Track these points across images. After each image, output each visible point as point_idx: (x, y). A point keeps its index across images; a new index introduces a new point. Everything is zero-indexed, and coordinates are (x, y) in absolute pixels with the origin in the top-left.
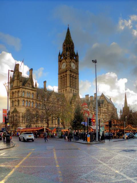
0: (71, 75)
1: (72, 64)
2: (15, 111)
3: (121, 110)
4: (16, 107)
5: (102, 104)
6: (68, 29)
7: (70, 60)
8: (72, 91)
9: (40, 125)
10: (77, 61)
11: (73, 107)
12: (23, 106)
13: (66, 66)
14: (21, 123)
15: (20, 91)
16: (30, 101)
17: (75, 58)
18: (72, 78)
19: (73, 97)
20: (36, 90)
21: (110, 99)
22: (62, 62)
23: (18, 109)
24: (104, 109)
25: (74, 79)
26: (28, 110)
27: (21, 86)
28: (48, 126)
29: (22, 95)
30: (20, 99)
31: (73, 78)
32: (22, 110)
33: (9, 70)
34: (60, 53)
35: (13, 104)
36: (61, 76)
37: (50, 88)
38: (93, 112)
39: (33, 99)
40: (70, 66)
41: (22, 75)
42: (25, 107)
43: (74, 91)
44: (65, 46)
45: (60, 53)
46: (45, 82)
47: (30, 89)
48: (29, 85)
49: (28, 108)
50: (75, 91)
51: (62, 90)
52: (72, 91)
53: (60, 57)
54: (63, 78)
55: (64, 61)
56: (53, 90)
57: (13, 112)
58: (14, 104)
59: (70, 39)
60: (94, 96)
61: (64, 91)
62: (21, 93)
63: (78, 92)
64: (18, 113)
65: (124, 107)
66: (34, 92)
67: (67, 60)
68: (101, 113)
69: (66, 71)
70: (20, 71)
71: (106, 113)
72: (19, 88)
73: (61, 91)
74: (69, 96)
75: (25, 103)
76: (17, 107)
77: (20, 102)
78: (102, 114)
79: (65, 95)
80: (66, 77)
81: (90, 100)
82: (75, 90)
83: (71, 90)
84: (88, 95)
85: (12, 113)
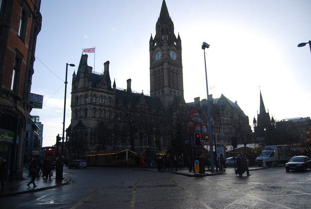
0: (170, 68)
1: (171, 54)
3: (254, 119)
5: (223, 110)
7: (169, 47)
8: (173, 92)
9: (120, 146)
10: (179, 48)
13: (163, 56)
15: (89, 94)
16: (104, 110)
17: (175, 44)
18: (171, 74)
20: (114, 92)
21: (236, 102)
23: (85, 122)
24: (226, 118)
27: (90, 88)
28: (132, 149)
29: (92, 100)
30: (88, 107)
32: (91, 123)
33: (67, 64)
34: (151, 37)
35: (77, 114)
36: (155, 71)
37: (136, 89)
39: (109, 106)
40: (169, 56)
41: (93, 70)
43: (175, 92)
45: (151, 37)
46: (129, 81)
48: (103, 85)
51: (157, 92)
52: (173, 92)
53: (152, 43)
54: (157, 73)
55: (158, 48)
57: (75, 127)
58: (78, 114)
61: (159, 92)
62: (90, 97)
65: (259, 113)
67: (164, 48)
68: (221, 125)
69: (162, 64)
70: (89, 64)
72: (88, 90)
73: (155, 94)
74: (168, 100)
75: (97, 113)
76: (83, 119)
78: (223, 126)
79: (162, 99)
80: (163, 72)
83: (171, 91)
84: (199, 98)
85: (74, 129)
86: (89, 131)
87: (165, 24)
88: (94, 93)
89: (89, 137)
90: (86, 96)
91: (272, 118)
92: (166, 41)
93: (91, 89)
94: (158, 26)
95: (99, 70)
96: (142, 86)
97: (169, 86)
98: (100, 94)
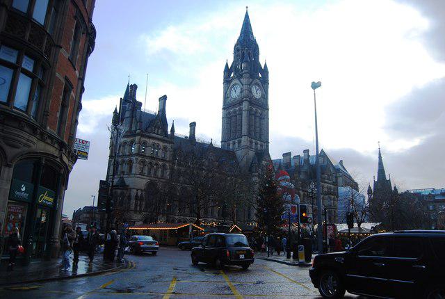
1: (254, 90)
2: (123, 185)
3: (370, 187)
4: (125, 176)
6: (247, 16)
7: (251, 80)
9: (177, 217)
10: (264, 82)
11: (256, 179)
12: (141, 174)
13: (241, 92)
14: (132, 212)
15: (137, 141)
17: (260, 76)
19: (254, 158)
21: (341, 162)
22: (232, 84)
23: (129, 181)
24: (326, 185)
25: (258, 119)
26: (151, 185)
29: (139, 150)
31: (255, 116)
32: (137, 182)
36: (230, 113)
38: (301, 192)
39: (163, 160)
40: (251, 92)
41: (143, 109)
42: (144, 177)
43: (256, 144)
44: (238, 51)
47: (158, 139)
48: (156, 130)
49: (152, 179)
50: (259, 145)
51: (231, 142)
55: (236, 81)
56: (210, 142)
58: (119, 169)
59: (251, 36)
60: (302, 155)
61: (234, 143)
63: (268, 146)
64: (127, 189)
66: (166, 144)
67: (244, 81)
69: (241, 103)
70: (139, 98)
71: (331, 194)
72: (135, 135)
77: (134, 165)
80: (241, 114)
81: (293, 164)
82: (259, 142)
83: (251, 142)
86: (133, 193)
87: (247, 47)
88: (143, 139)
89: (133, 201)
90: (132, 143)
91: (395, 188)
92: (246, 71)
93: (138, 134)
94: (236, 50)
95: (150, 106)
96: (211, 131)
97: (249, 135)
98: (152, 141)
